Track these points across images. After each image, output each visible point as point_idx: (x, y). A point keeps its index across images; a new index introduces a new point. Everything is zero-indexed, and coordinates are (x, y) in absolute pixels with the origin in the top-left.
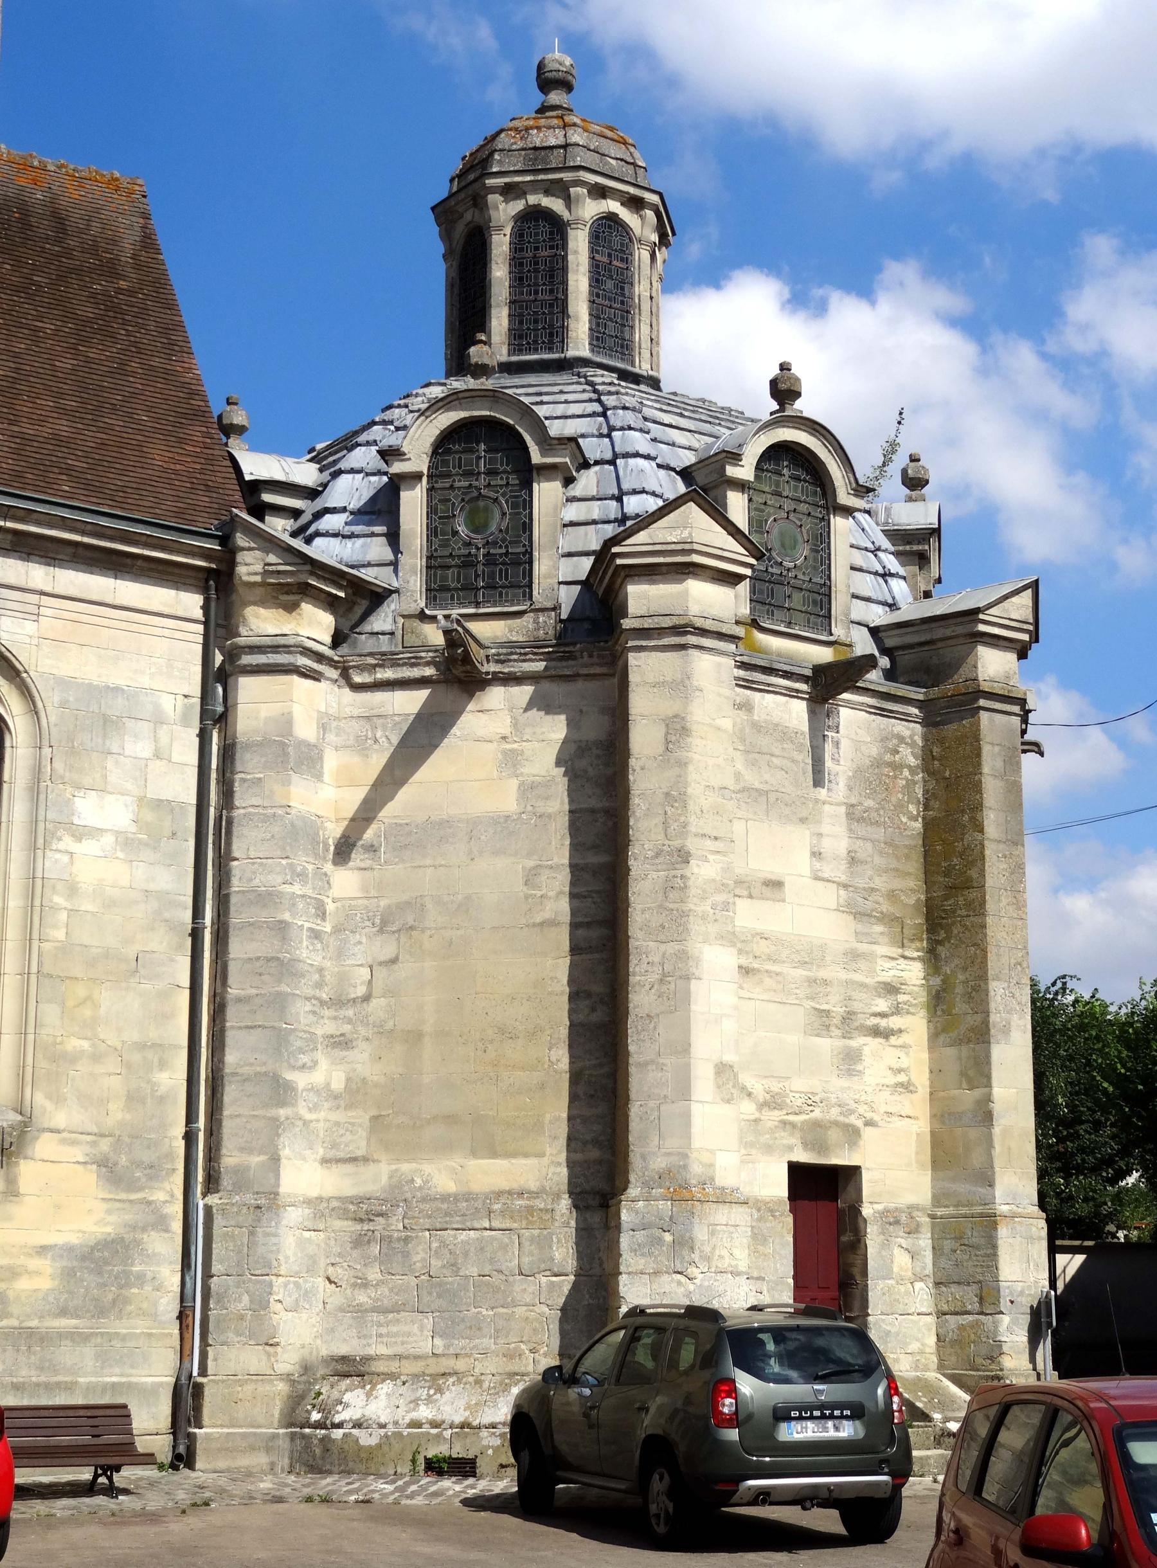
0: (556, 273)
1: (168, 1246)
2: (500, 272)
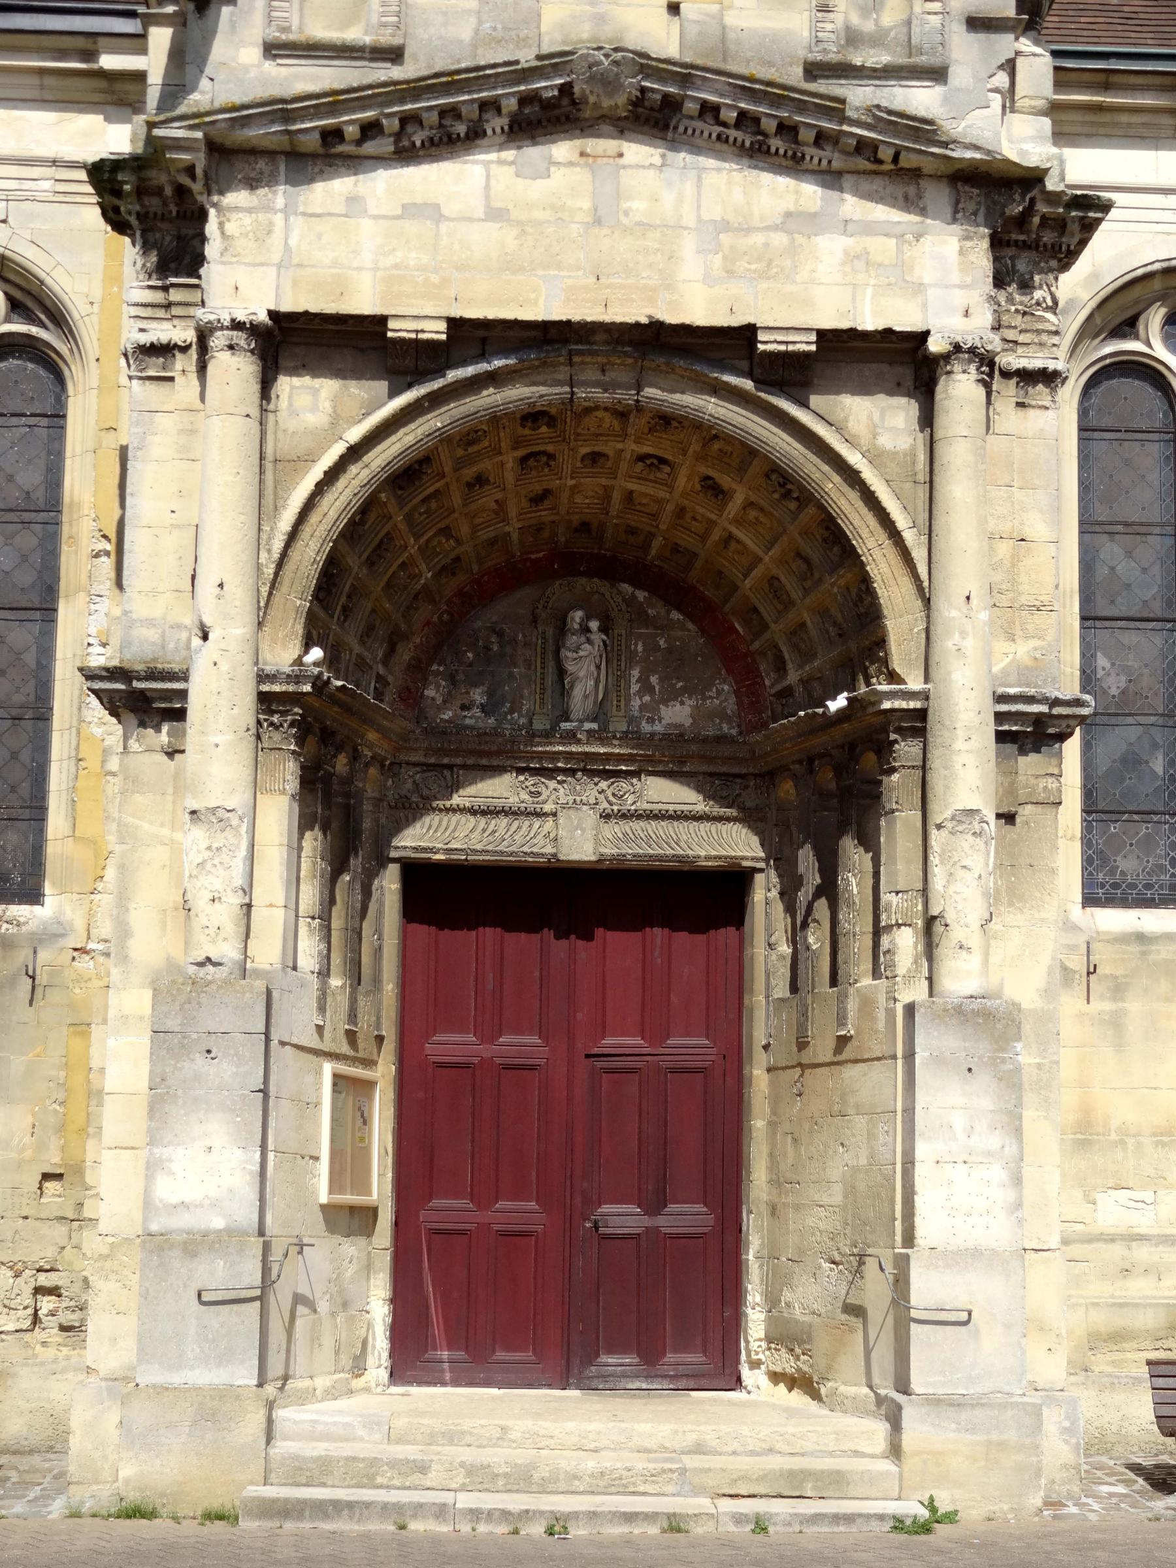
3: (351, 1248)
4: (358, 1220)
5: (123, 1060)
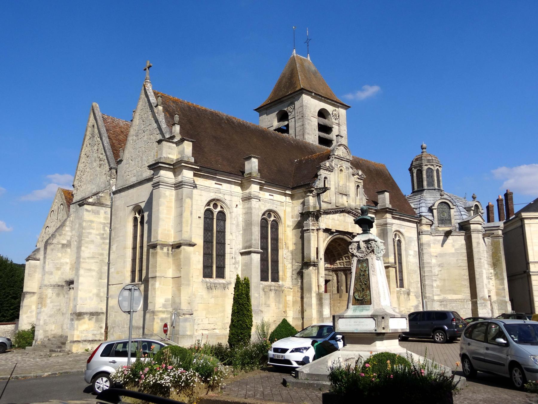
0: (432, 177)
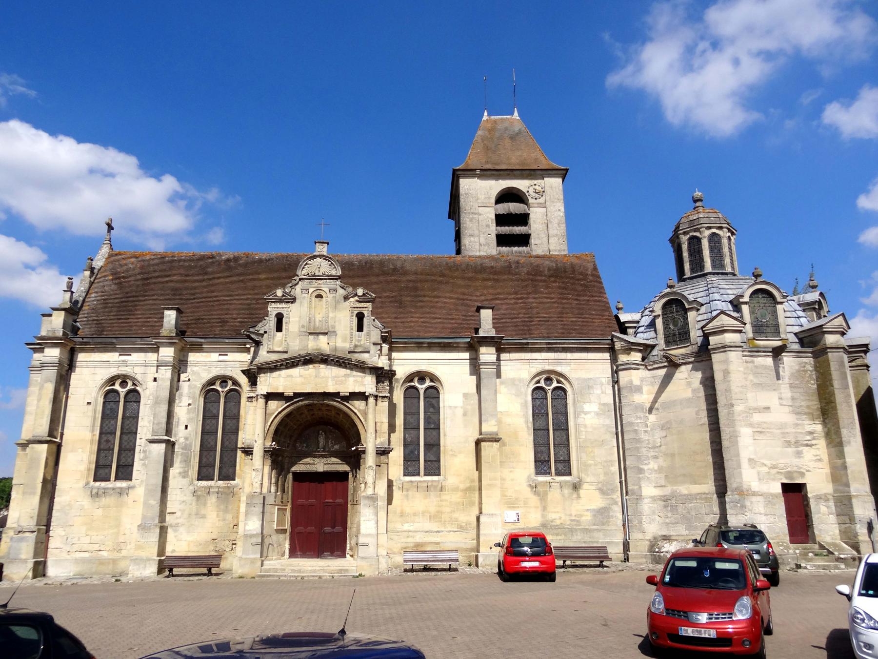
0: (700, 251)
1: (618, 509)
2: (685, 254)
3: (282, 536)
4: (284, 531)
5: (243, 508)
